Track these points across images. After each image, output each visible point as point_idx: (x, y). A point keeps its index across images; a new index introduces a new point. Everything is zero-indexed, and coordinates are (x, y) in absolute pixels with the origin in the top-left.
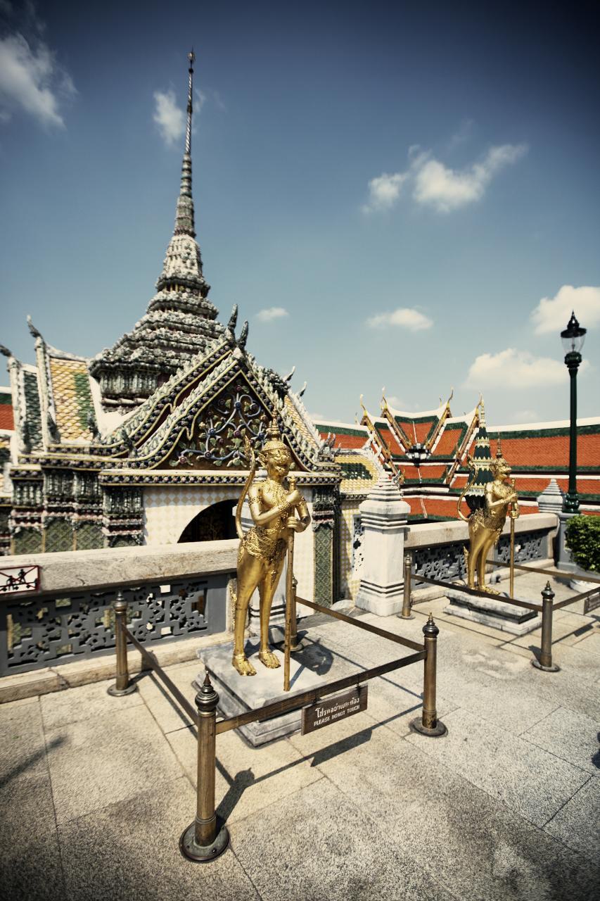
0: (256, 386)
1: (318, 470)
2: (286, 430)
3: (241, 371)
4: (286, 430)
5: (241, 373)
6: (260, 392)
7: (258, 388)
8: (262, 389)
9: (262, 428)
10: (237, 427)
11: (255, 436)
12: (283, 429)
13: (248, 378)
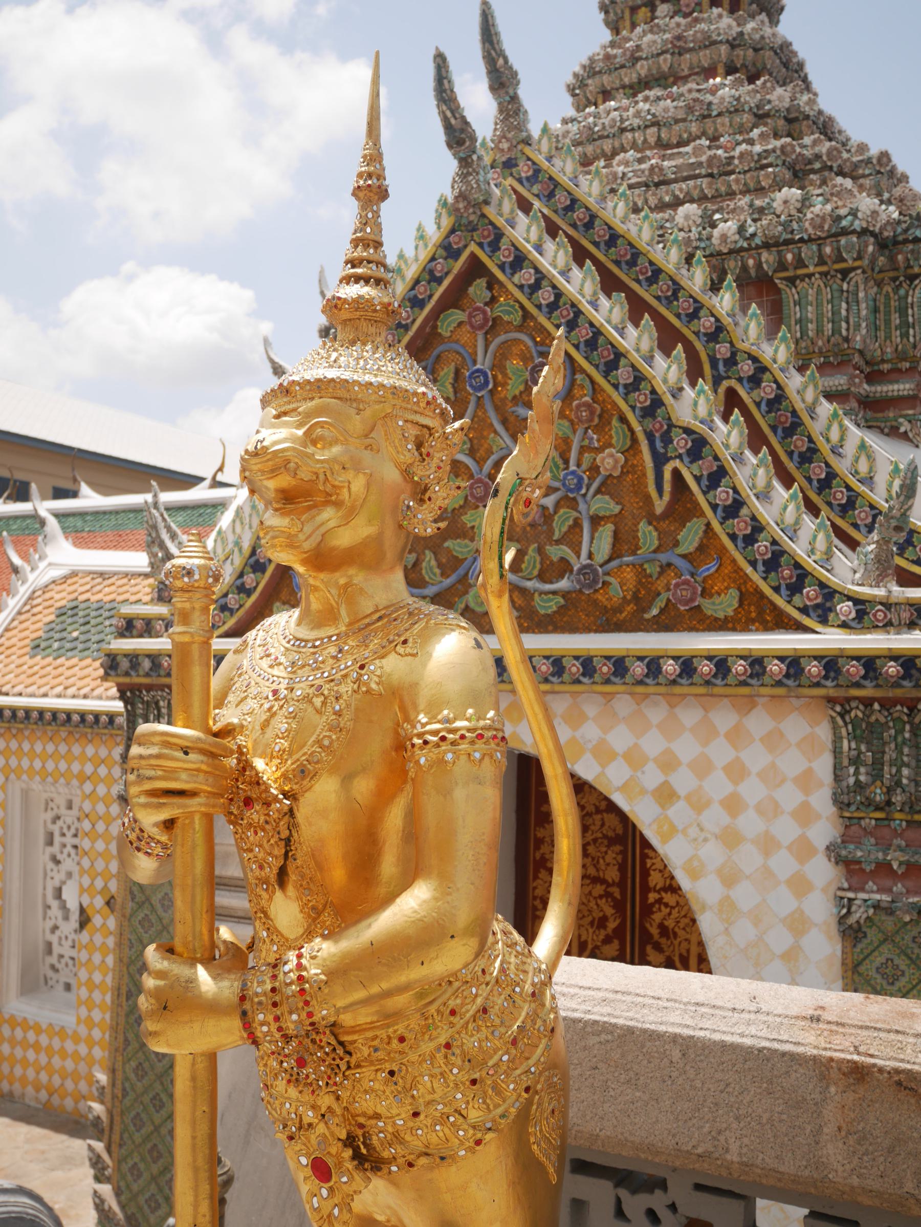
0: (536, 287)
1: (864, 615)
2: (681, 443)
3: (473, 247)
4: (681, 443)
5: (473, 256)
6: (553, 307)
7: (545, 296)
8: (559, 295)
9: (582, 450)
10: (480, 462)
11: (556, 490)
12: (667, 439)
13: (502, 267)
